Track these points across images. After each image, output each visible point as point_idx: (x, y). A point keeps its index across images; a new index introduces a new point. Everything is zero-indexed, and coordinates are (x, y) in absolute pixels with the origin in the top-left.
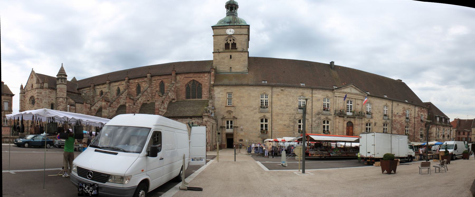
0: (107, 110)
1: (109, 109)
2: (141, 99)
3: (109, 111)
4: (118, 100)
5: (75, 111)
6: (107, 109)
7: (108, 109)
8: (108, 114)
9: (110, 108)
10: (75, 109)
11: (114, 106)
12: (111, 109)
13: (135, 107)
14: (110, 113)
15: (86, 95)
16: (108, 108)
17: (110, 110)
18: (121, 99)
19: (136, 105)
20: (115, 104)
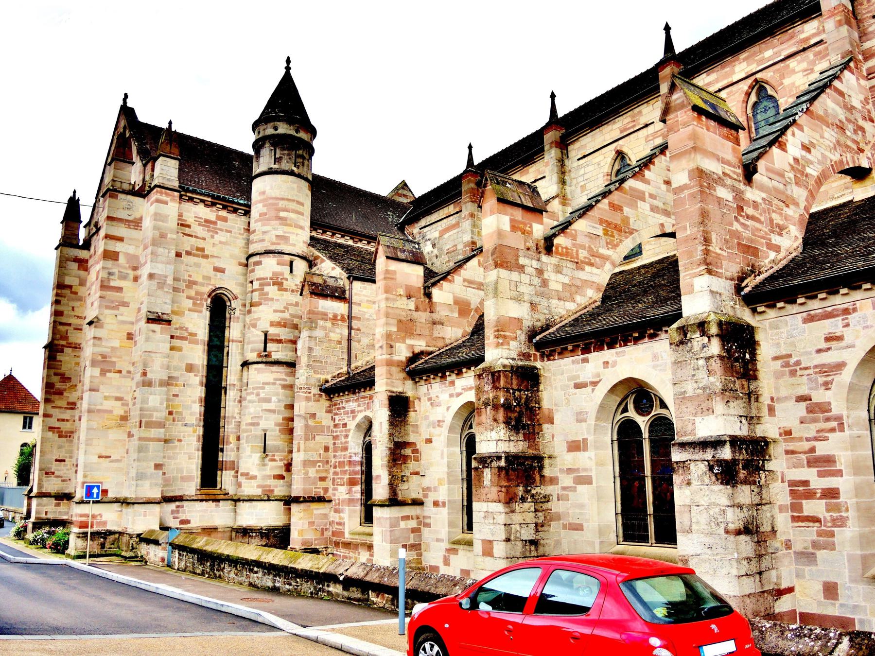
0: (525, 278)
1: (540, 272)
2: (806, 148)
3: (545, 283)
4: (616, 208)
5: (350, 328)
6: (521, 268)
7: (528, 270)
8: (533, 306)
9: (544, 258)
10: (350, 317)
11: (583, 247)
12: (558, 270)
13: (755, 205)
14: (554, 302)
15: (440, 249)
16: (535, 264)
17: (549, 275)
18: (634, 206)
19: (762, 188)
20: (591, 236)
